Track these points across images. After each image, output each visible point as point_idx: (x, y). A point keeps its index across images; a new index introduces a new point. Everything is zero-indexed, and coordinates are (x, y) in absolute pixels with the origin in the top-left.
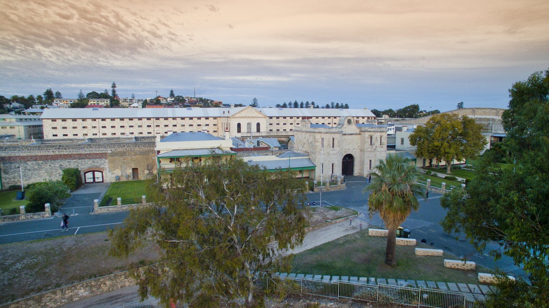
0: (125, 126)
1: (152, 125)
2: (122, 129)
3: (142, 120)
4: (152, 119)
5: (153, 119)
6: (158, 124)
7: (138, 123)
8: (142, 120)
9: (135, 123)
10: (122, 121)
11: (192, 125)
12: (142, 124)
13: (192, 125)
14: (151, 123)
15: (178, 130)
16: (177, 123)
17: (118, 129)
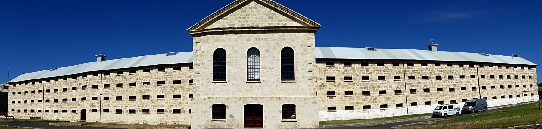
1: (99, 85)
6: (107, 82)
11: (162, 82)
13: (162, 82)
14: (98, 82)
15: (137, 93)
16: (137, 79)
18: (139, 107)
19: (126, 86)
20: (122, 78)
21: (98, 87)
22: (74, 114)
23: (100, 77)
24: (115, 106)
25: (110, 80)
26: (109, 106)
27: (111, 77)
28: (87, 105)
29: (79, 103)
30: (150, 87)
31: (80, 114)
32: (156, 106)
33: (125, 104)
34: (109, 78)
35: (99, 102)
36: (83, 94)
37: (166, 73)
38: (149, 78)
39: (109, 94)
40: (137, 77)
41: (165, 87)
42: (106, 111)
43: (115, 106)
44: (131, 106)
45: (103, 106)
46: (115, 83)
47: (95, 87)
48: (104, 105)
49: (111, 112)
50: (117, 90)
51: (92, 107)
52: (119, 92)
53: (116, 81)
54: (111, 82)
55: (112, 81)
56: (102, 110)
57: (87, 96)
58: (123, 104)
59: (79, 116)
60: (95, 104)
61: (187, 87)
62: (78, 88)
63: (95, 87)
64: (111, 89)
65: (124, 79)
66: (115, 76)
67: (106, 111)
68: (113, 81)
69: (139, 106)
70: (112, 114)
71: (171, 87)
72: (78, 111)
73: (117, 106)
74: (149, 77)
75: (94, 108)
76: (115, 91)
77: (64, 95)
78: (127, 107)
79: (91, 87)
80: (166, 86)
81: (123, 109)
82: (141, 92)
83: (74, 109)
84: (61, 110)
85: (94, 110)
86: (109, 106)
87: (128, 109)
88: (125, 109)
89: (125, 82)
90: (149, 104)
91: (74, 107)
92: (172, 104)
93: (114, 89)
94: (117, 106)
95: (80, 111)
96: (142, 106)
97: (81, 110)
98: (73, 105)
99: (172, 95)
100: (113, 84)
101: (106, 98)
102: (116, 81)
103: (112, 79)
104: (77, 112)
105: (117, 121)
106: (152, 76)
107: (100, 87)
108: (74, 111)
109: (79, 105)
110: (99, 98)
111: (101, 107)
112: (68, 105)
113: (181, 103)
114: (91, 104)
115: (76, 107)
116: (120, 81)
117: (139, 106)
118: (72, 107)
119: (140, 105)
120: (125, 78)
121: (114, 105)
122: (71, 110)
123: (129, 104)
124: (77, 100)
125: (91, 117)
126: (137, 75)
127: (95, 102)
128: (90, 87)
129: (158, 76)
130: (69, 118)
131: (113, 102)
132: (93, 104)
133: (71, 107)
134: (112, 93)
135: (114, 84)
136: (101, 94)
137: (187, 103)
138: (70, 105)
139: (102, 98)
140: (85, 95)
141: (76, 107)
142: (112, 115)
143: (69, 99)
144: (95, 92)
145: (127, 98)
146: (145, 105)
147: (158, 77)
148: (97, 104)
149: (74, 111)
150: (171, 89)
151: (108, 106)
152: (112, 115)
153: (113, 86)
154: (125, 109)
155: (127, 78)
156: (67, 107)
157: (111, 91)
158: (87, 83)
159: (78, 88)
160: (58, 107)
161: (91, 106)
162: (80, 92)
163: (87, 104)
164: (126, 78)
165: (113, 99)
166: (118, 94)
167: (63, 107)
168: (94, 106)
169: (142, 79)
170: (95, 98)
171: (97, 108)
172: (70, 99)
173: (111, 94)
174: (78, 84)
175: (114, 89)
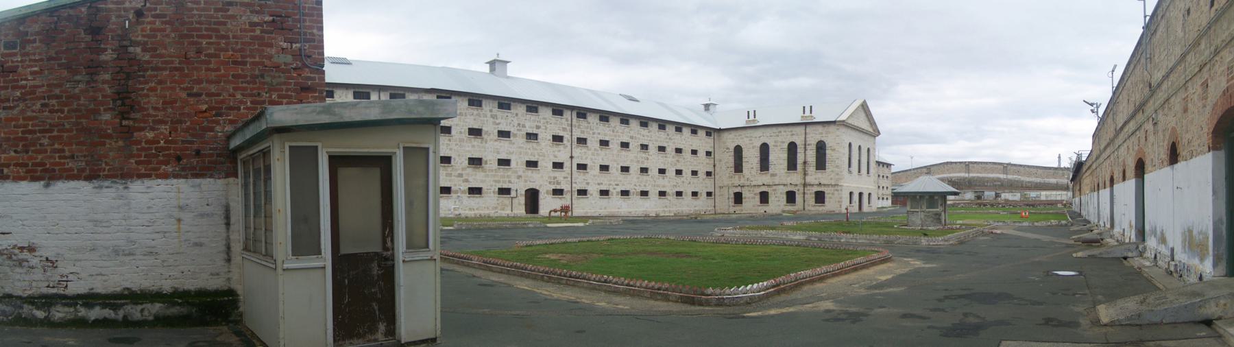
0: (484, 129)
1: (566, 136)
2: (476, 142)
3: (536, 111)
4: (567, 114)
5: (569, 112)
6: (583, 132)
7: (527, 124)
8: (536, 111)
9: (516, 123)
10: (474, 111)
12: (538, 127)
14: (564, 129)
15: (632, 161)
16: (632, 137)
17: (461, 140)
18: (636, 188)
19: (615, 146)
20: (608, 129)
21: (565, 141)
22: (505, 200)
23: (567, 120)
24: (599, 184)
25: (589, 130)
26: (588, 184)
27: (589, 123)
28: (542, 180)
29: (520, 173)
30: (650, 154)
31: (522, 200)
32: (658, 186)
33: (614, 181)
34: (586, 125)
35: (568, 174)
36: (530, 152)
37: (668, 135)
38: (649, 139)
39: (586, 158)
40: (632, 133)
41: (666, 157)
42: (582, 192)
43: (599, 184)
44: (623, 185)
45: (576, 183)
46: (597, 138)
47: (558, 139)
48: (577, 181)
49: (592, 195)
50: (600, 151)
51: (554, 184)
52: (604, 157)
53: (599, 134)
54: (590, 134)
55: (591, 132)
56: (575, 191)
57: (541, 158)
58: (611, 180)
59: (519, 204)
60: (560, 179)
61: (689, 160)
62: (515, 135)
63: (558, 139)
64: (590, 150)
65: (611, 133)
66: (597, 124)
67: (582, 192)
68: (594, 133)
69: (635, 185)
70: (594, 200)
71: (673, 157)
72: (517, 191)
73: (602, 184)
74: (648, 136)
75: (558, 187)
76: (598, 154)
77: (473, 146)
78: (617, 185)
79: (550, 140)
80: (668, 156)
81: (611, 190)
82: (638, 162)
83: (505, 186)
84: (465, 187)
85: (558, 192)
86: (588, 184)
87: (619, 189)
88: (614, 189)
89: (613, 139)
90: (649, 182)
91: (504, 182)
92: (675, 184)
93: (595, 150)
94: (602, 184)
95: (524, 193)
96: (640, 185)
97: (527, 191)
98: (503, 177)
99: (674, 169)
100: (593, 139)
101: (582, 167)
102: (599, 134)
103: (591, 129)
104: (513, 194)
105: (603, 212)
106: (651, 135)
107: (568, 141)
108: (504, 191)
109: (519, 177)
110: (567, 165)
111: (574, 185)
112: (487, 176)
113: (683, 182)
114: (550, 177)
115: (510, 182)
116: (605, 135)
117: (635, 185)
118: (499, 182)
119: (637, 185)
120: (613, 131)
121: (596, 182)
122: (497, 190)
123: (621, 181)
124: (513, 164)
125: (547, 204)
126: (631, 130)
127: (559, 174)
128: (546, 139)
129: (658, 137)
130: (490, 208)
131: (594, 176)
132: (555, 178)
133: (496, 181)
134: (593, 157)
135: (596, 139)
136: (572, 157)
137: (690, 183)
138: (494, 176)
139: (575, 167)
140: (537, 157)
141: (510, 182)
142: (593, 202)
143: (490, 160)
144: (560, 151)
145: (617, 170)
146: (644, 184)
147: (659, 140)
148: (565, 178)
149: (504, 191)
150: (673, 160)
151: (585, 183)
152: (593, 202)
153: (593, 143)
154: (614, 189)
155: (617, 132)
156: (482, 181)
157: (590, 152)
158: (538, 127)
159: (515, 135)
160: (453, 178)
161: (550, 183)
162: (522, 145)
163: (542, 177)
164: (615, 131)
165: (594, 170)
166: (603, 160)
167: (470, 179)
168: (558, 183)
169: (639, 139)
170: (558, 166)
171: (565, 186)
172: (491, 158)
173: (592, 159)
174: (516, 125)
175: (595, 150)
